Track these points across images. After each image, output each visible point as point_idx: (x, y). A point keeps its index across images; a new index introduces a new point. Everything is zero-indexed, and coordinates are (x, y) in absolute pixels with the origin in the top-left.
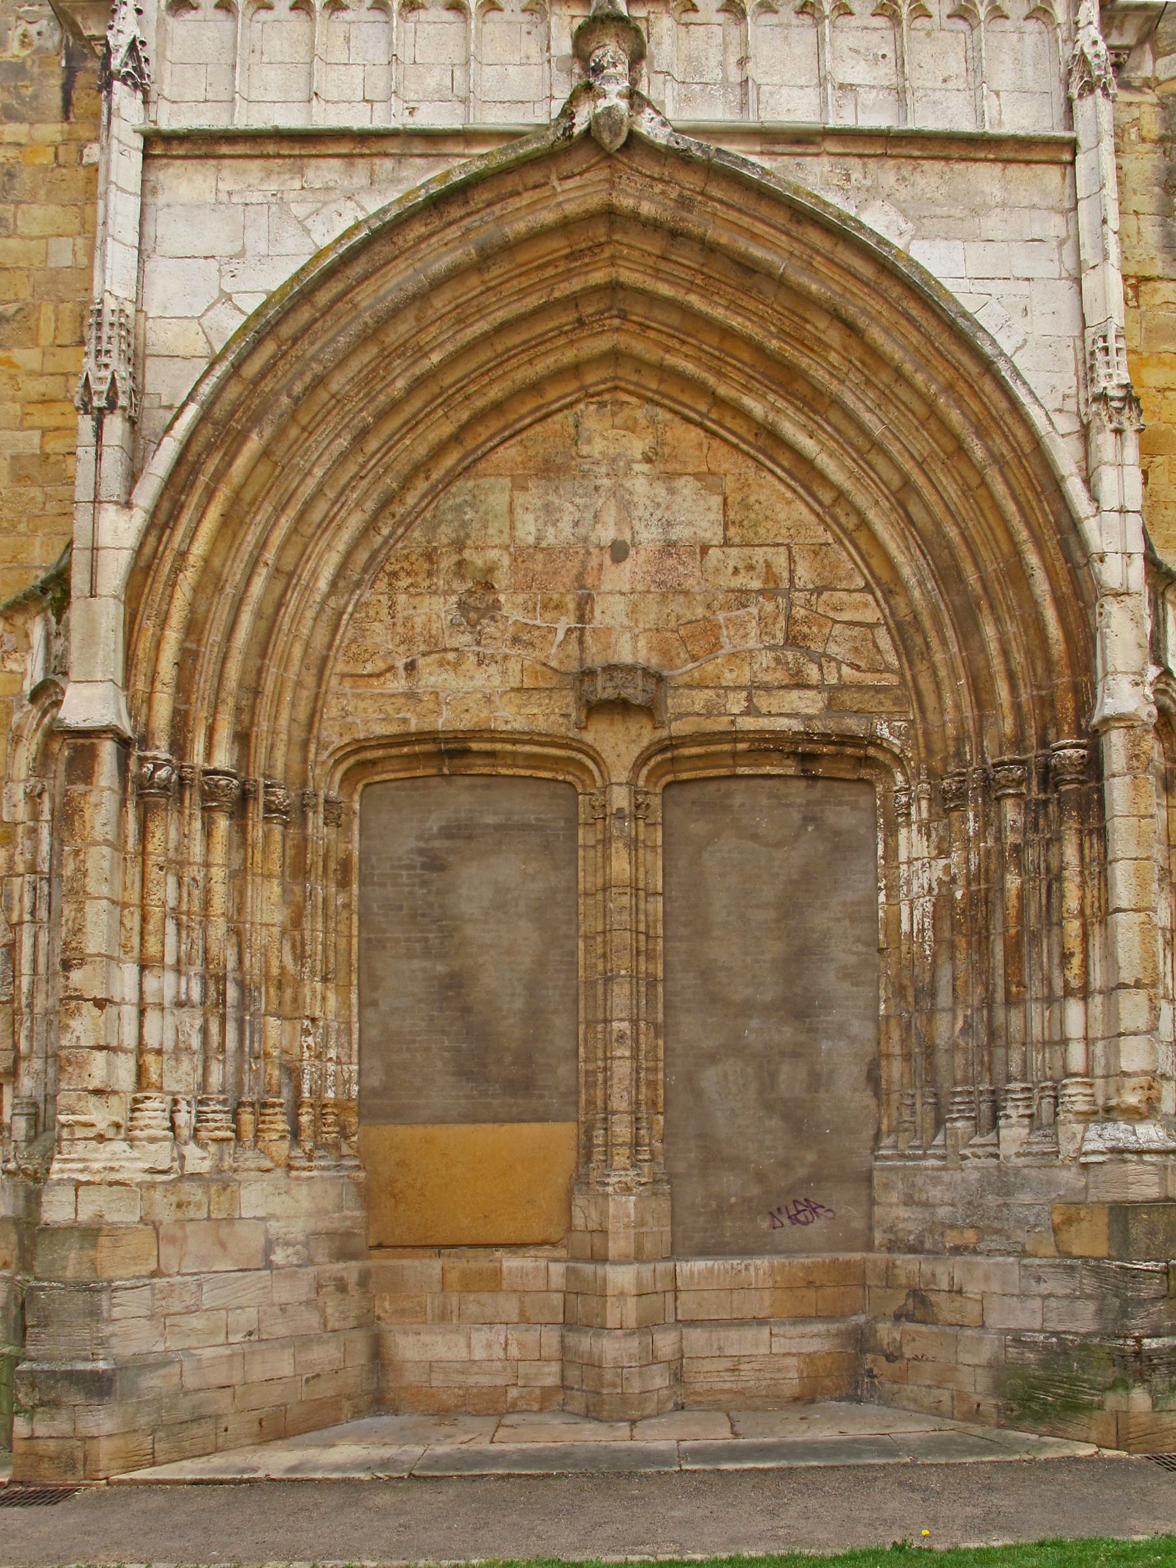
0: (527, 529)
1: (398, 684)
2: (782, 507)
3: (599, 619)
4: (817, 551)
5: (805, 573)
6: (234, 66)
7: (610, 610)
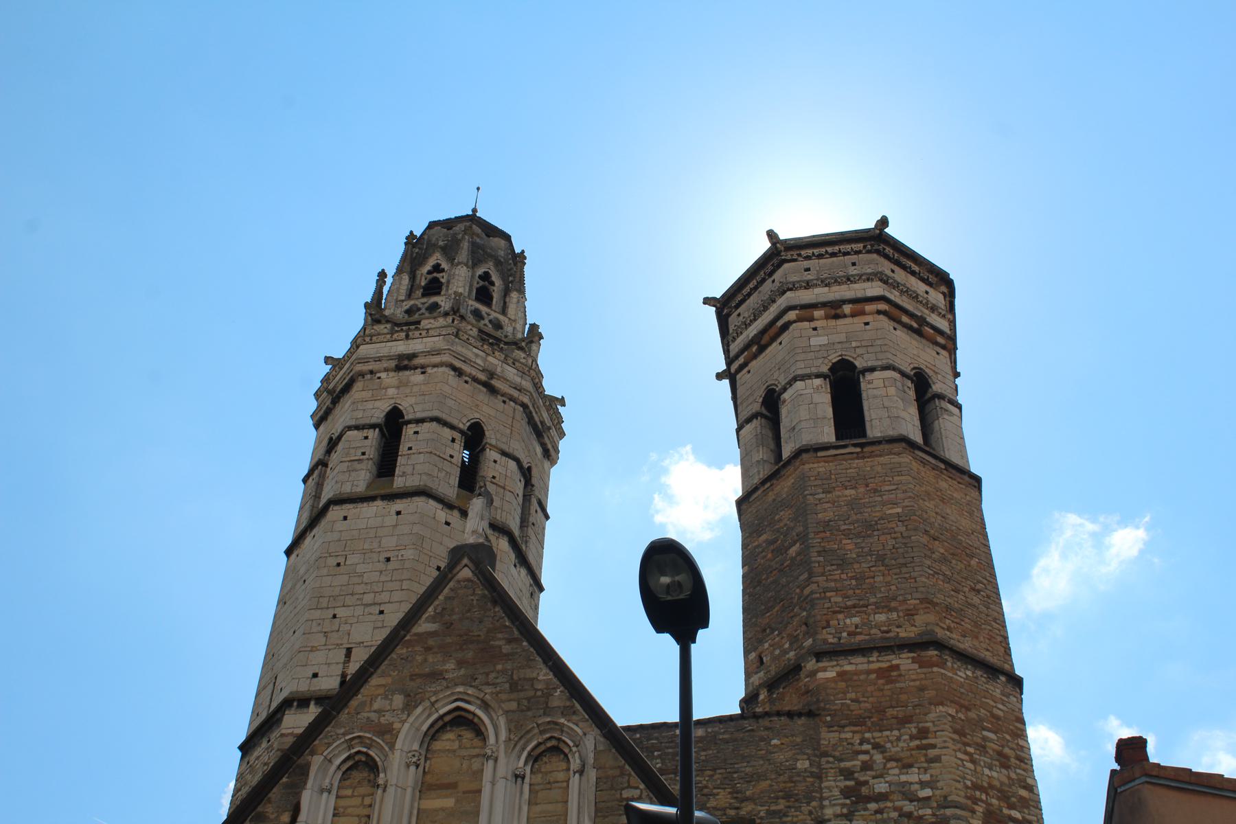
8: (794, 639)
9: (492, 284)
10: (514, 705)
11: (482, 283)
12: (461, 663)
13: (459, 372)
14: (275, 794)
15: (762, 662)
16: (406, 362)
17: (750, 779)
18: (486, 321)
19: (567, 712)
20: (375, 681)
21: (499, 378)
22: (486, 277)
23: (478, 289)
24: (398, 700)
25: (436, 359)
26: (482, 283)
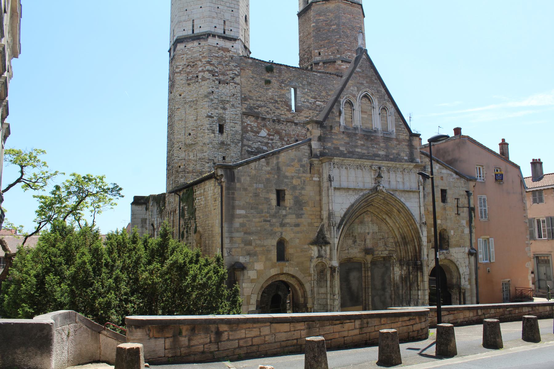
0: (359, 230)
1: (347, 251)
2: (384, 227)
3: (367, 242)
4: (387, 233)
5: (386, 236)
6: (340, 176)
7: (368, 241)
8: (333, 53)
10: (378, 96)
12: (367, 82)
14: (335, 107)
15: (320, 54)
17: (330, 90)
19: (388, 101)
20: (350, 82)
24: (356, 88)
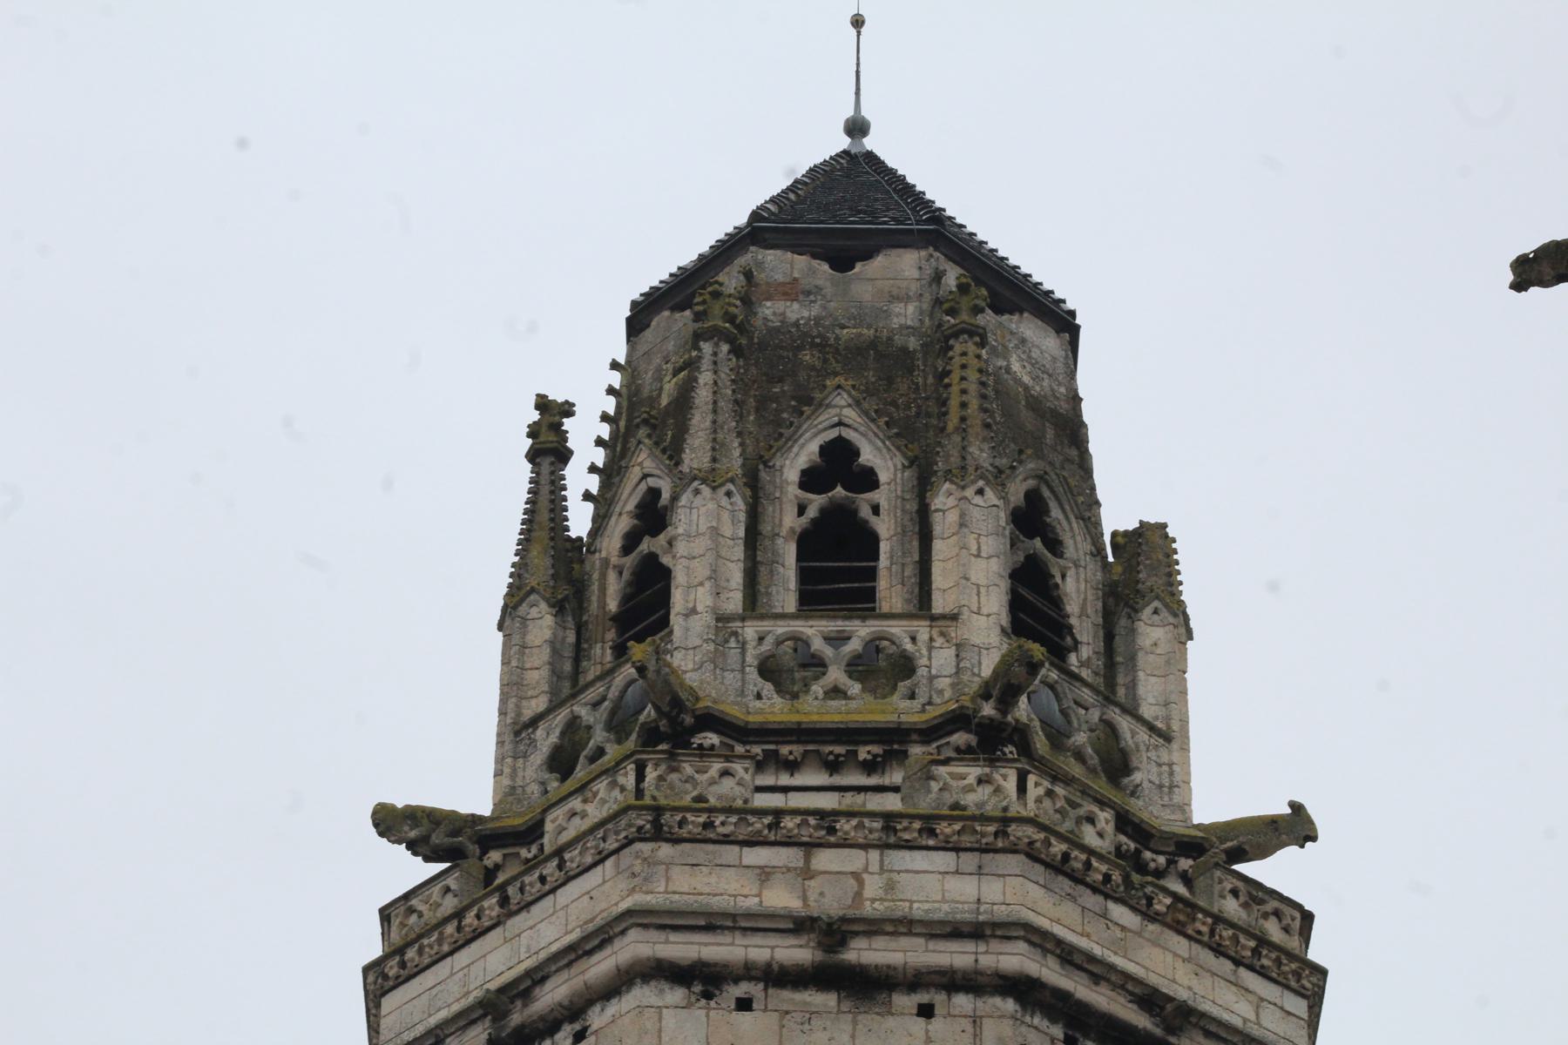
9: (867, 480)
11: (816, 502)
13: (703, 980)
16: (516, 1019)
18: (836, 675)
21: (874, 927)
22: (838, 466)
23: (808, 543)
25: (601, 966)
26: (816, 502)
